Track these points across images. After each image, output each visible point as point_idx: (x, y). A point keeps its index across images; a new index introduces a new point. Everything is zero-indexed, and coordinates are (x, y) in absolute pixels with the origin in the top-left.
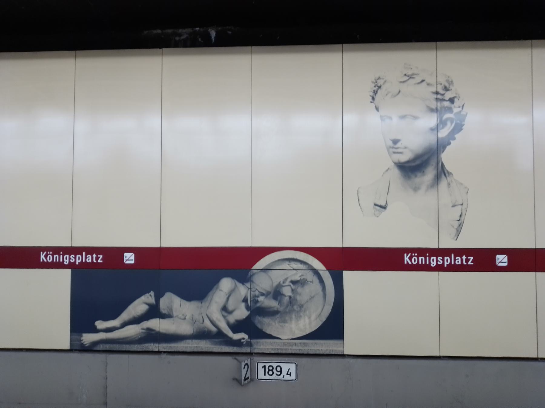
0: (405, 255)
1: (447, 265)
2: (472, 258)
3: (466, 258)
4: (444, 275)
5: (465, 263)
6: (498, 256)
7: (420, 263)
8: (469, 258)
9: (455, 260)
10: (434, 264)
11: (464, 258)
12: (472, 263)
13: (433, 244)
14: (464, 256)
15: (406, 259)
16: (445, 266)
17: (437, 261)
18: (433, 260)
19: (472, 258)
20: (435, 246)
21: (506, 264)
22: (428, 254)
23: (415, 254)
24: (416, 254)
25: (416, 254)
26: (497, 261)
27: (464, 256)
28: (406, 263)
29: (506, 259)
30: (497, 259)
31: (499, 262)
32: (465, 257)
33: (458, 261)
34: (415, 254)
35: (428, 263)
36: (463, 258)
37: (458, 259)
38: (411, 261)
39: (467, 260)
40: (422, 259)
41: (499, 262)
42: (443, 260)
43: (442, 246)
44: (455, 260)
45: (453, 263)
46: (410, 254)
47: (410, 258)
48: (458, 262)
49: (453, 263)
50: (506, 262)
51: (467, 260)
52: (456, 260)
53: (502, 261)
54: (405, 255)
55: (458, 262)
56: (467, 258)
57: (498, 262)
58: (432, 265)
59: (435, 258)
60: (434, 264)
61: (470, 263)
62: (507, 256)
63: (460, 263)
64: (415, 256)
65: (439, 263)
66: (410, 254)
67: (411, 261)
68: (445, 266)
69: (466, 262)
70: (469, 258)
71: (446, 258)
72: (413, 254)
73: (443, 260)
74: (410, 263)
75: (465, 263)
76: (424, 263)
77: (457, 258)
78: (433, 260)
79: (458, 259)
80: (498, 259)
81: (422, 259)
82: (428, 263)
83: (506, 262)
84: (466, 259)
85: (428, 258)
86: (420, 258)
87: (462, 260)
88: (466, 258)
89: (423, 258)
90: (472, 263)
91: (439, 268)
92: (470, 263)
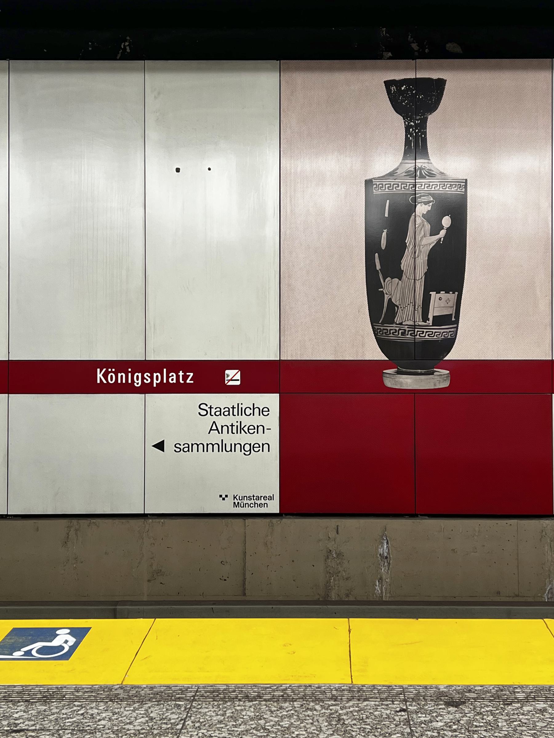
0: (98, 370)
1: (157, 383)
2: (192, 374)
3: (183, 374)
4: (152, 398)
5: (181, 381)
6: (227, 372)
7: (119, 382)
8: (188, 374)
9: (168, 377)
10: (138, 383)
11: (181, 374)
12: (192, 382)
13: (137, 355)
14: (181, 372)
15: (100, 375)
16: (155, 385)
17: (143, 378)
18: (138, 377)
19: (192, 374)
20: (139, 357)
21: (238, 383)
22: (130, 370)
23: (112, 370)
24: (113, 370)
25: (113, 370)
26: (226, 379)
27: (181, 372)
28: (99, 382)
29: (238, 376)
30: (226, 376)
31: (229, 380)
32: (182, 372)
33: (173, 379)
34: (112, 370)
35: (130, 382)
36: (179, 374)
37: (173, 376)
38: (106, 379)
39: (185, 377)
40: (122, 376)
41: (229, 380)
42: (152, 377)
43: (151, 357)
44: (168, 377)
45: (165, 381)
46: (104, 370)
47: (105, 376)
48: (172, 380)
49: (165, 381)
50: (238, 380)
51: (185, 377)
52: (171, 377)
53: (233, 379)
54: (98, 370)
55: (172, 380)
56: (185, 374)
57: (227, 380)
58: (135, 384)
59: (140, 375)
60: (138, 383)
61: (188, 381)
62: (240, 372)
63: (175, 381)
64: (112, 372)
65: (145, 381)
66: (104, 370)
67: (106, 379)
68: (155, 385)
69: (183, 380)
70: (188, 374)
71: (155, 375)
72: (110, 370)
73: (152, 377)
74: (105, 382)
75: (181, 381)
76: (124, 382)
77: (170, 375)
78: (138, 377)
79: (173, 376)
80: (228, 376)
81: (122, 376)
82: (130, 382)
83: (238, 380)
84: (182, 375)
85: (130, 374)
86: (119, 375)
87: (178, 377)
88: (183, 374)
89: (124, 375)
90: (192, 382)
91: (146, 389)
92: (188, 381)
